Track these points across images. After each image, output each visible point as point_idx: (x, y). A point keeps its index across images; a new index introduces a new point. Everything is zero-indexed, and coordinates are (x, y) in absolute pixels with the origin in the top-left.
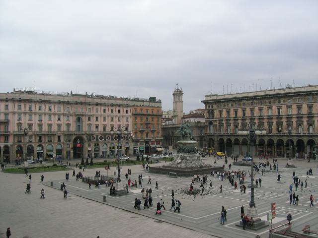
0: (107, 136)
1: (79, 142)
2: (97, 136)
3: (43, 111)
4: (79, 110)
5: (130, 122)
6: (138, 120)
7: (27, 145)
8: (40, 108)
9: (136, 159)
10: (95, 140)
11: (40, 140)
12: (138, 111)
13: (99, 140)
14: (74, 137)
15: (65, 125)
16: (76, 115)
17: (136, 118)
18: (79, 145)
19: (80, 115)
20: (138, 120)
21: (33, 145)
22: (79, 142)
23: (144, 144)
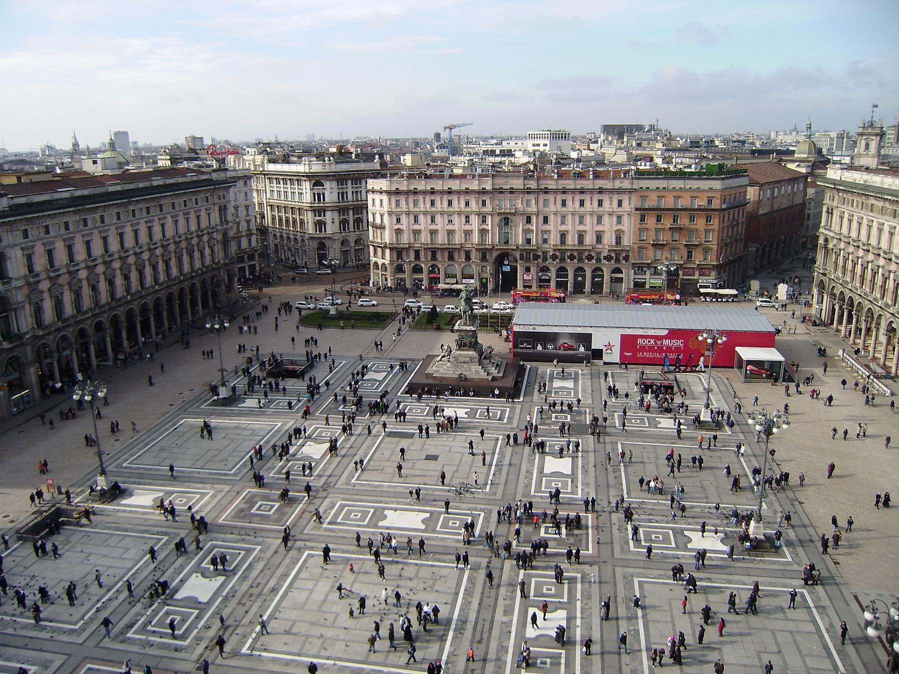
1: (506, 262)
4: (506, 205)
5: (628, 225)
6: (651, 222)
7: (412, 265)
9: (224, 388)
10: (540, 260)
11: (434, 258)
12: (652, 201)
14: (495, 254)
16: (499, 214)
17: (643, 219)
18: (507, 269)
19: (508, 213)
20: (651, 222)
21: (423, 266)
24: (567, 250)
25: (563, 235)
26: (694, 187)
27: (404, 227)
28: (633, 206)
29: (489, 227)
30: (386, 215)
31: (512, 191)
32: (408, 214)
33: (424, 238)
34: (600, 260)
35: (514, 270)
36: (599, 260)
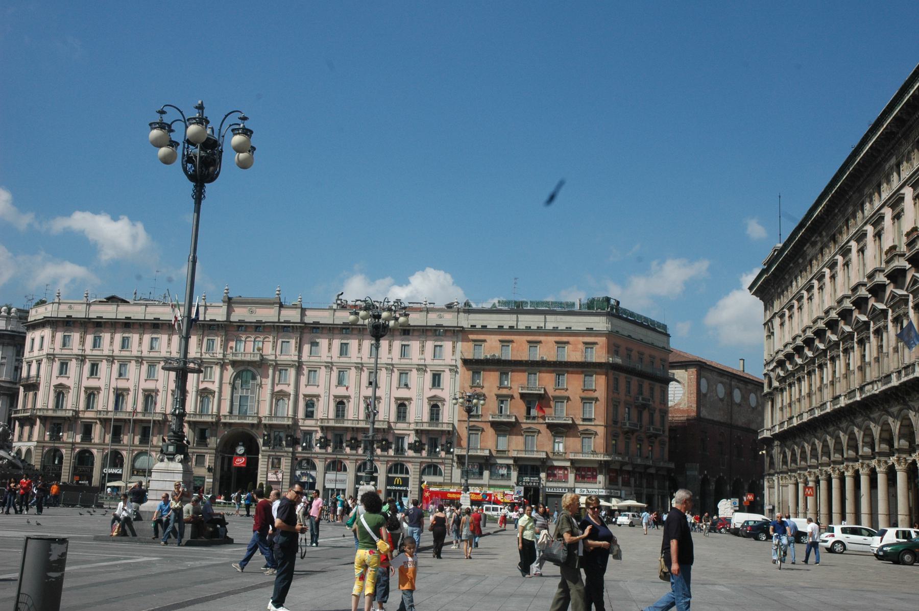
0: (348, 436)
1: (240, 450)
2: (309, 433)
3: (134, 350)
8: (125, 344)
12: (491, 348)
13: (317, 449)
15: (194, 393)
18: (240, 462)
22: (240, 450)
23: (514, 474)
24: (347, 429)
25: (341, 403)
26: (562, 327)
27: (70, 382)
28: (458, 356)
29: (215, 387)
30: (45, 360)
31: (259, 327)
32: (82, 359)
33: (104, 402)
34: (403, 450)
35: (253, 464)
36: (400, 450)
